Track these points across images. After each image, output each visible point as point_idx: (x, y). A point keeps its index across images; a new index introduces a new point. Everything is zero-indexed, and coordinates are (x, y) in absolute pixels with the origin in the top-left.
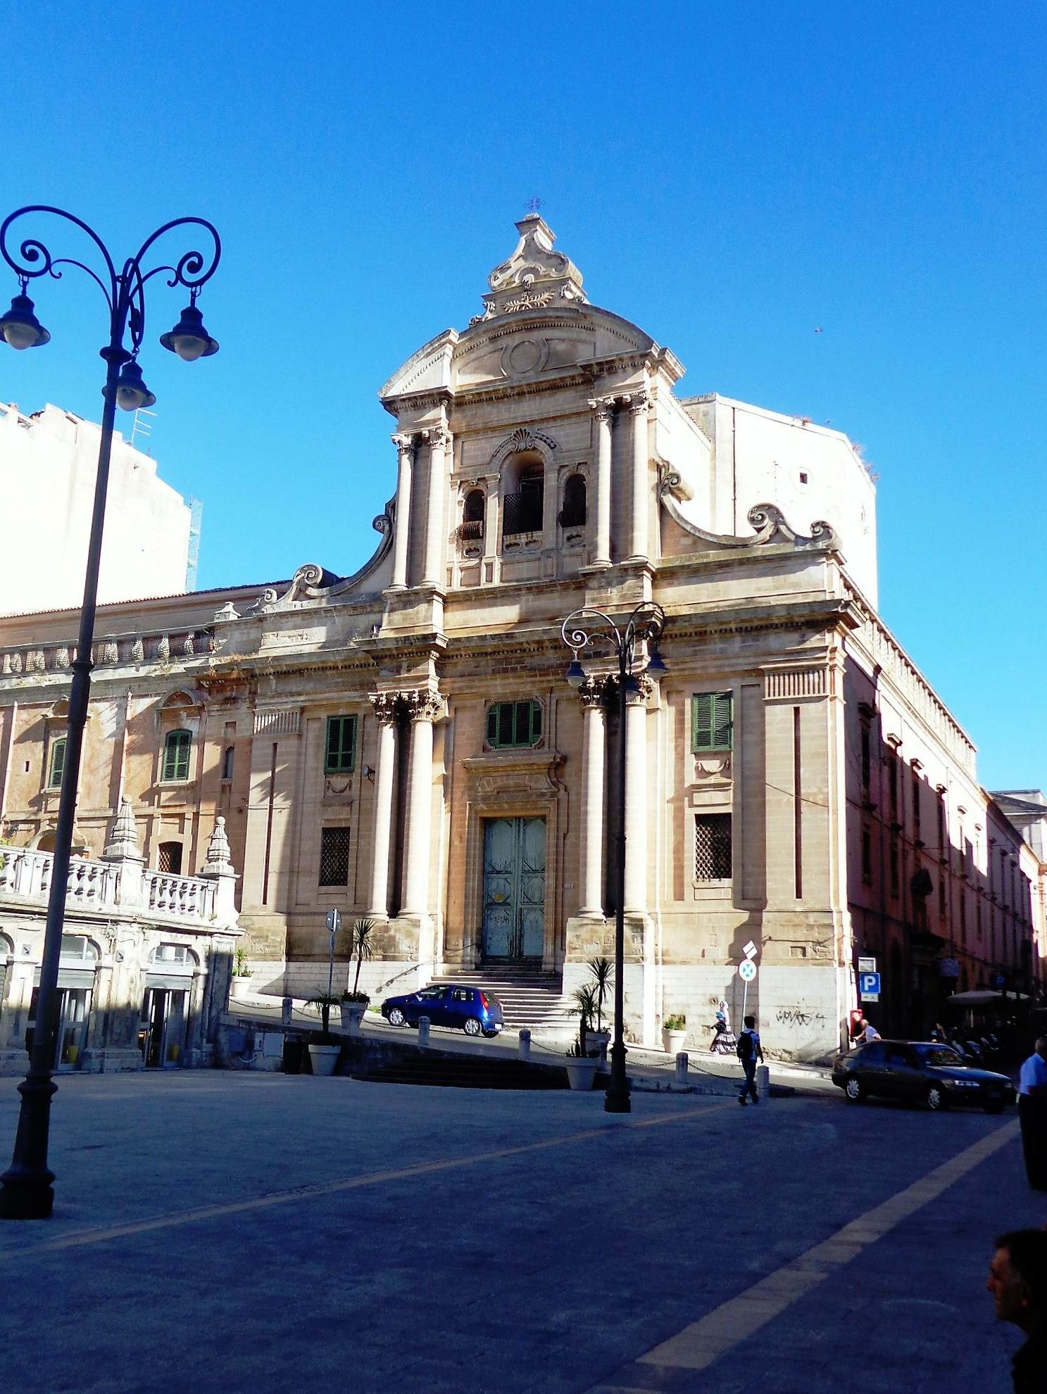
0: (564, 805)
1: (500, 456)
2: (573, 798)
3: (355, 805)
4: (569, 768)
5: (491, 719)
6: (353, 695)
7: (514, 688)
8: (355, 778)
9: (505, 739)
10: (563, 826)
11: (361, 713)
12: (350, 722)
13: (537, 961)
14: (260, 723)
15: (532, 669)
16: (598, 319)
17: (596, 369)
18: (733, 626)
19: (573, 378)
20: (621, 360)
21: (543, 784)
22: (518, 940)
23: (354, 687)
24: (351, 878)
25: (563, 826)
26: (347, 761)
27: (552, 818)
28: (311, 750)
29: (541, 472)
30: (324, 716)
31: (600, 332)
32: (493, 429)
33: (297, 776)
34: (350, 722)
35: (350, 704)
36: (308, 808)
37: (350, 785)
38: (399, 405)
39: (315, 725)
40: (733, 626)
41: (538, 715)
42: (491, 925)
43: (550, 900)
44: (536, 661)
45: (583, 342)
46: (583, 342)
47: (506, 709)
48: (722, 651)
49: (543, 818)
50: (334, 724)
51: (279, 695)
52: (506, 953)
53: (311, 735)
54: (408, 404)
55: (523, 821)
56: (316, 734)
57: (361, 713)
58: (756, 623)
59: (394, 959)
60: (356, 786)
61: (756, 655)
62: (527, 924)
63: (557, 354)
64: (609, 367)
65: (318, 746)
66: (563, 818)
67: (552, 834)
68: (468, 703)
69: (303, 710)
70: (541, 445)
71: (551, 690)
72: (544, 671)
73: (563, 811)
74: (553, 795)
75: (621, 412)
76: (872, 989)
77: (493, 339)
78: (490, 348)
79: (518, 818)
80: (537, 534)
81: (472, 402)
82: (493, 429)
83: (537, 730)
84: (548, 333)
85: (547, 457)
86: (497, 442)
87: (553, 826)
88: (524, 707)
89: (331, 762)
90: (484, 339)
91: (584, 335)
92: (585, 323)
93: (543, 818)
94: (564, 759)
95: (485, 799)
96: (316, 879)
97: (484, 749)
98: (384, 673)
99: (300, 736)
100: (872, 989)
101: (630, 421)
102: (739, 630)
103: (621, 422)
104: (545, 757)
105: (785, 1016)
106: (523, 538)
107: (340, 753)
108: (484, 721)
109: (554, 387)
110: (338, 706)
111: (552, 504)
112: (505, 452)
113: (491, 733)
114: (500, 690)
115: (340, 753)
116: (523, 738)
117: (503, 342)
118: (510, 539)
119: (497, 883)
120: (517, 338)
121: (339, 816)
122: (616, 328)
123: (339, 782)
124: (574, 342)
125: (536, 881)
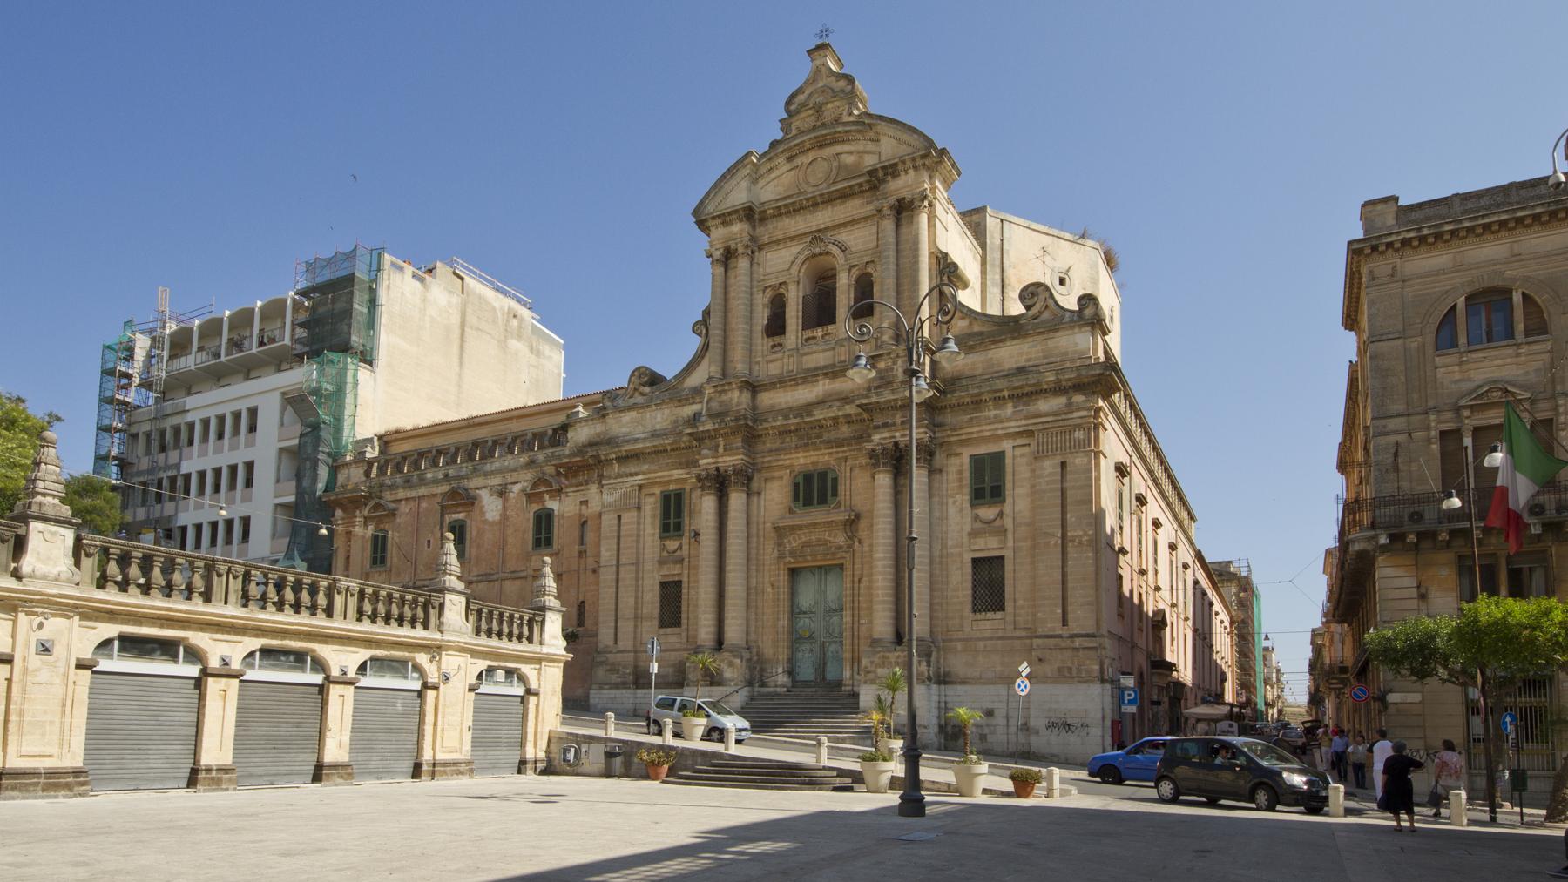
0: (858, 555)
1: (799, 262)
2: (866, 549)
3: (686, 563)
4: (863, 524)
5: (796, 486)
6: (678, 473)
7: (815, 459)
8: (685, 540)
9: (808, 502)
10: (858, 572)
11: (688, 488)
12: (679, 496)
13: (839, 684)
14: (610, 497)
15: (829, 442)
16: (882, 128)
17: (881, 173)
18: (1006, 393)
19: (860, 185)
20: (904, 162)
21: (840, 538)
22: (821, 667)
23: (680, 465)
24: (684, 621)
25: (858, 572)
26: (678, 527)
27: (848, 565)
28: (648, 520)
29: (834, 277)
30: (657, 491)
31: (884, 140)
32: (792, 239)
33: (638, 542)
34: (679, 496)
35: (677, 481)
36: (648, 567)
38: (710, 223)
39: (652, 499)
40: (1006, 393)
41: (835, 480)
42: (799, 655)
43: (847, 634)
44: (833, 435)
45: (868, 153)
46: (868, 153)
47: (808, 478)
48: (996, 416)
49: (841, 566)
50: (666, 497)
51: (621, 476)
52: (812, 678)
53: (648, 507)
54: (718, 221)
55: (824, 570)
56: (652, 506)
57: (688, 488)
58: (1027, 389)
59: (720, 684)
60: (685, 547)
61: (1027, 418)
62: (829, 654)
63: (846, 166)
64: (892, 170)
65: (654, 516)
66: (858, 566)
67: (848, 580)
68: (776, 474)
69: (641, 487)
70: (834, 249)
71: (846, 460)
72: (839, 443)
73: (858, 560)
74: (850, 546)
75: (904, 210)
76: (1131, 702)
77: (789, 159)
78: (788, 166)
79: (820, 567)
80: (831, 328)
81: (772, 217)
82: (792, 239)
83: (835, 494)
84: (838, 148)
85: (840, 260)
86: (795, 250)
87: (849, 573)
88: (823, 475)
89: (665, 528)
90: (782, 159)
91: (870, 146)
92: (871, 134)
93: (841, 566)
94: (858, 516)
95: (791, 552)
96: (656, 623)
97: (791, 511)
98: (705, 452)
99: (639, 508)
100: (1131, 702)
101: (912, 220)
102: (1011, 397)
103: (904, 221)
104: (842, 516)
105: (1052, 726)
106: (819, 332)
107: (672, 521)
108: (789, 489)
109: (844, 196)
110: (668, 483)
111: (844, 300)
112: (802, 257)
113: (796, 498)
114: (802, 461)
115: (672, 521)
116: (823, 500)
117: (798, 161)
118: (809, 333)
119: (804, 622)
120: (810, 156)
121: (672, 571)
122: (899, 134)
123: (672, 545)
124: (861, 153)
125: (836, 619)
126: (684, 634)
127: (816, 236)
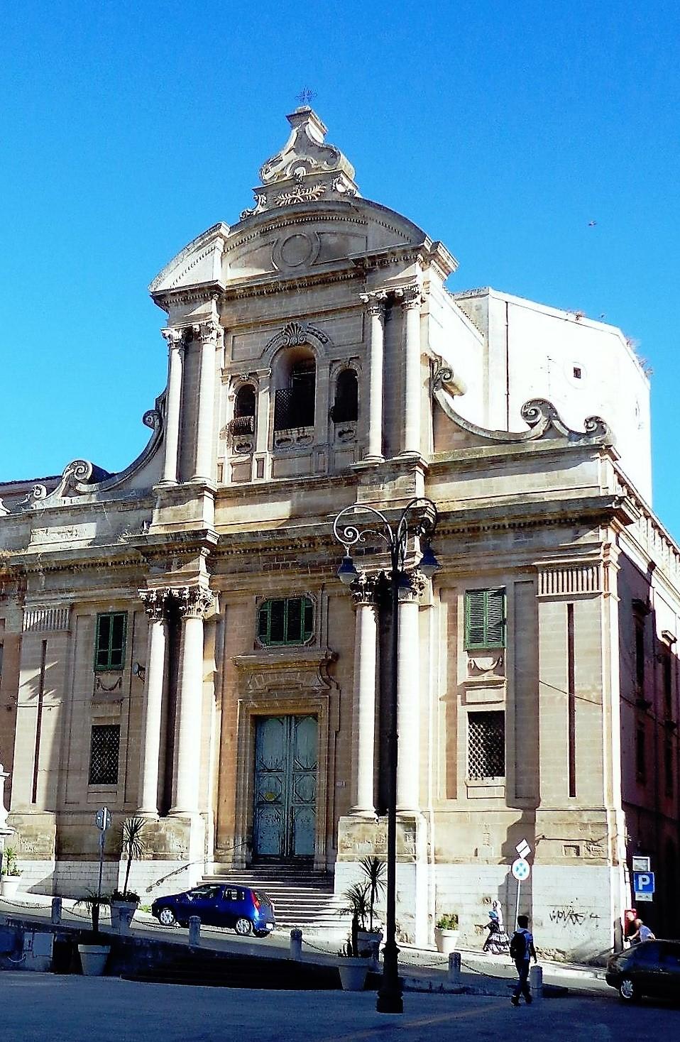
0: (335, 702)
1: (272, 351)
2: (344, 695)
3: (126, 703)
4: (341, 666)
5: (263, 616)
6: (123, 592)
7: (285, 585)
8: (126, 675)
9: (277, 636)
10: (335, 724)
11: (131, 610)
12: (119, 620)
13: (309, 860)
14: (30, 620)
15: (304, 566)
16: (370, 212)
17: (367, 264)
18: (506, 522)
19: (345, 272)
20: (393, 253)
21: (315, 682)
23: (123, 583)
24: (121, 776)
25: (335, 724)
26: (117, 658)
27: (324, 715)
28: (80, 648)
29: (312, 367)
30: (94, 613)
32: (264, 324)
33: (67, 674)
34: (119, 620)
36: (78, 706)
38: (169, 299)
39: (85, 622)
40: (506, 522)
41: (309, 612)
44: (308, 558)
45: (355, 235)
46: (355, 235)
47: (277, 606)
48: (495, 547)
49: (315, 716)
50: (104, 622)
51: (49, 591)
53: (81, 632)
56: (86, 631)
57: (131, 610)
58: (529, 519)
59: (164, 858)
60: (126, 684)
61: (530, 552)
62: (298, 822)
64: (380, 261)
65: (87, 643)
66: (335, 716)
68: (239, 600)
69: (72, 607)
70: (313, 340)
71: (323, 587)
72: (316, 567)
73: (335, 709)
74: (325, 692)
75: (393, 307)
76: (646, 888)
78: (261, 241)
79: (290, 716)
80: (308, 429)
82: (264, 324)
83: (309, 627)
84: (320, 227)
85: (319, 352)
86: (268, 336)
87: (325, 724)
88: (295, 605)
89: (102, 659)
90: (256, 232)
91: (356, 229)
92: (358, 216)
93: (315, 716)
94: (336, 656)
96: (86, 777)
97: (256, 646)
98: (154, 569)
99: (70, 633)
100: (646, 888)
101: (403, 316)
102: (512, 526)
103: (393, 316)
104: (317, 655)
106: (294, 433)
107: (110, 650)
108: (255, 618)
109: (326, 281)
110: (108, 603)
111: (324, 399)
113: (262, 629)
115: (110, 650)
116: (294, 635)
117: (274, 237)
118: (282, 434)
119: (268, 781)
120: (289, 232)
121: (109, 714)
122: (388, 222)
123: (109, 679)
126: (121, 792)
127: (292, 323)
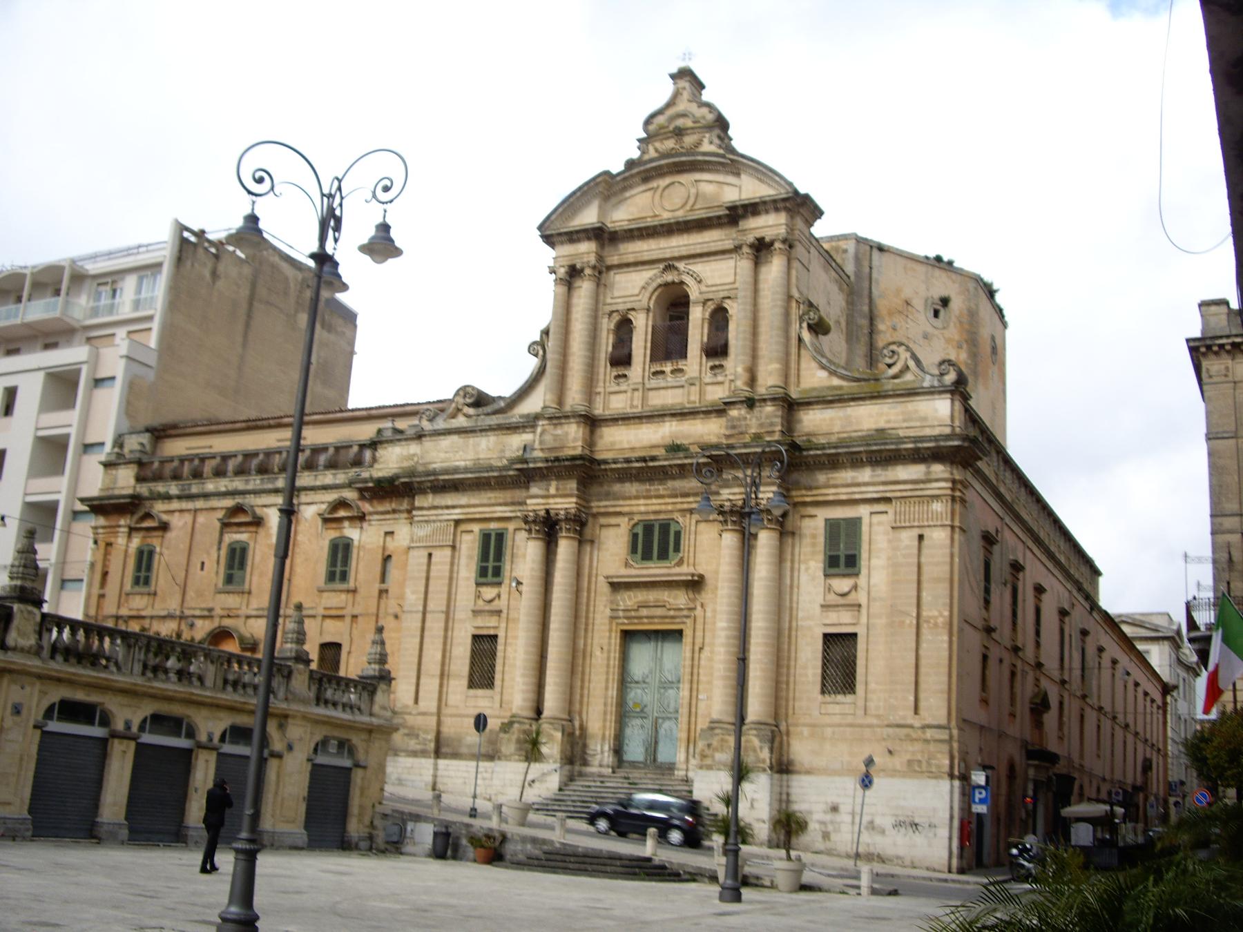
0: (700, 621)
1: (651, 289)
2: (709, 614)
3: (504, 615)
5: (635, 536)
8: (504, 589)
9: (647, 556)
10: (699, 641)
17: (740, 211)
22: (652, 747)
24: (497, 682)
26: (497, 572)
37: (855, 587)
41: (678, 534)
42: (628, 731)
43: (684, 711)
50: (486, 537)
52: (641, 758)
54: (565, 238)
56: (469, 544)
60: (504, 596)
62: (662, 732)
65: (470, 557)
66: (699, 634)
69: (457, 522)
73: (699, 626)
76: (982, 801)
83: (677, 549)
85: (694, 292)
88: (665, 527)
89: (483, 572)
96: (465, 682)
105: (898, 825)
106: (668, 368)
107: (491, 564)
113: (634, 550)
121: (487, 624)
123: (489, 592)
126: (497, 698)
127: (669, 265)
